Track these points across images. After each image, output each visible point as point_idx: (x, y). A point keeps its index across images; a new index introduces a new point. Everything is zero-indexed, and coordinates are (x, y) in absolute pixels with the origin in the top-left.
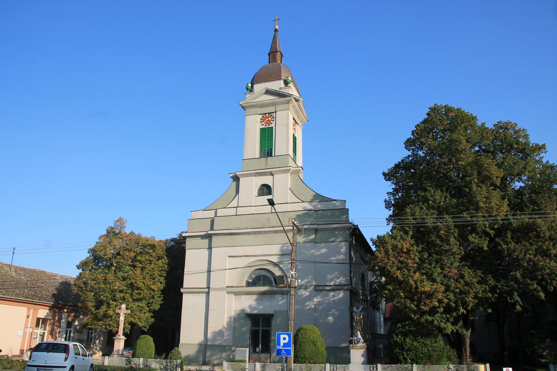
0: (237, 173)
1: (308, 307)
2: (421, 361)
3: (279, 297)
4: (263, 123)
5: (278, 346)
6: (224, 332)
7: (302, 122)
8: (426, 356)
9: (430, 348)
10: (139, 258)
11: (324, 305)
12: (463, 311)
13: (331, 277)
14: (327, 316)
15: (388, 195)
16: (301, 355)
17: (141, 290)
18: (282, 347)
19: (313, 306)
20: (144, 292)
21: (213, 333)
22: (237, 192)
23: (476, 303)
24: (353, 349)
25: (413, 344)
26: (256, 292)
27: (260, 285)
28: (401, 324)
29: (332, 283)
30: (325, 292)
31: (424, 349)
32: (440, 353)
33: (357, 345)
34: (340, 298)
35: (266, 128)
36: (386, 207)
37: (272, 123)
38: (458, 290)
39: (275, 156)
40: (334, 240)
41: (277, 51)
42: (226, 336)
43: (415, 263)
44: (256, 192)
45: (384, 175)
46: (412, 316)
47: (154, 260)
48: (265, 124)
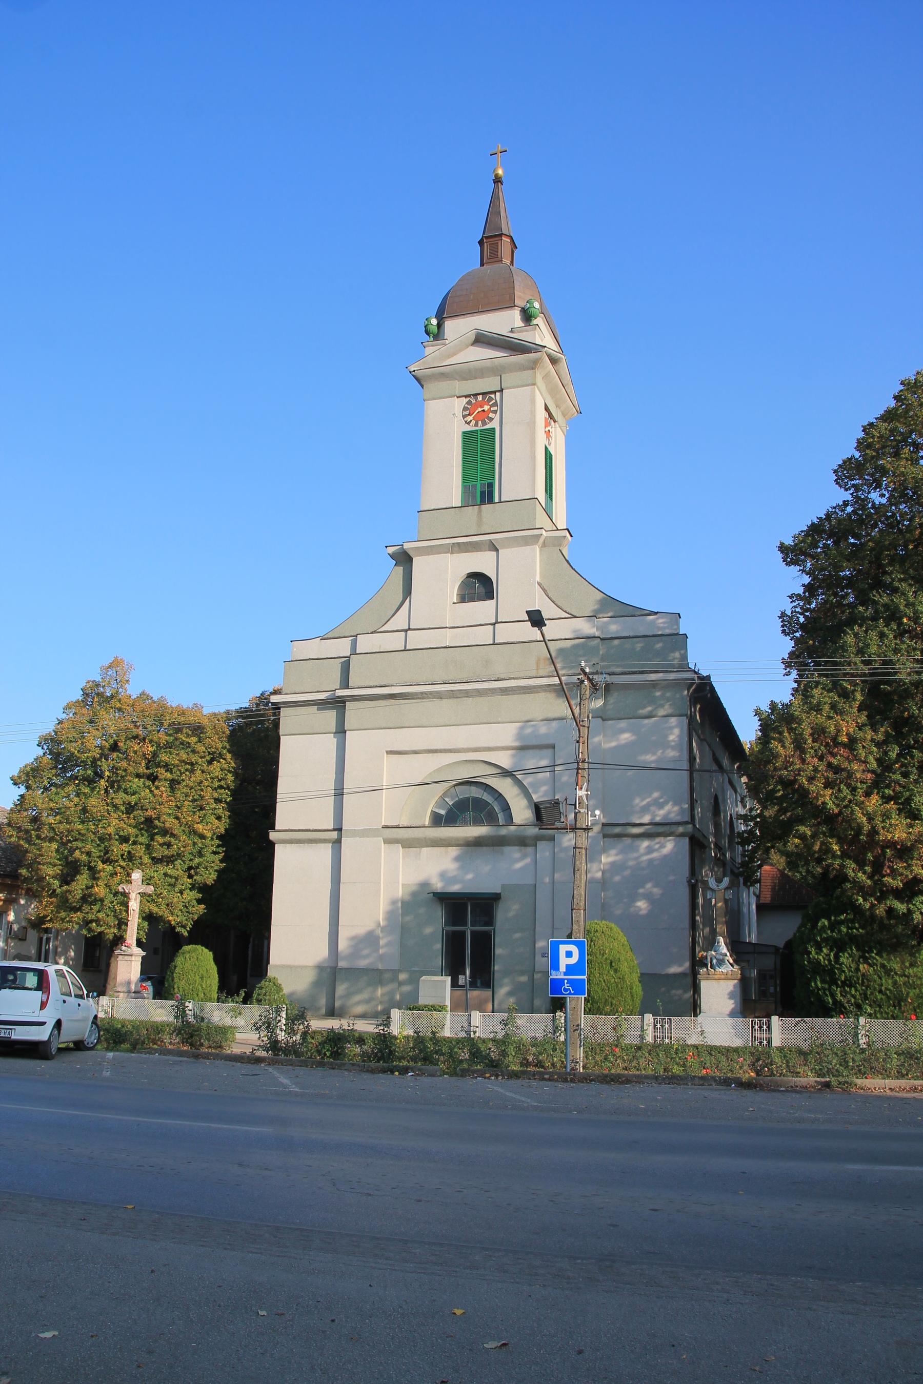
3: (514, 852)
4: (469, 418)
5: (553, 972)
6: (378, 938)
7: (564, 417)
8: (889, 998)
9: (900, 980)
10: (164, 757)
11: (627, 873)
13: (644, 803)
14: (634, 898)
15: (791, 602)
17: (173, 835)
18: (562, 974)
19: (599, 875)
20: (180, 841)
21: (352, 938)
22: (407, 591)
24: (707, 979)
25: (858, 970)
26: (457, 839)
27: (465, 823)
28: (829, 920)
29: (646, 819)
30: (628, 841)
31: (884, 981)
33: (718, 969)
34: (665, 856)
35: (477, 431)
36: (783, 631)
37: (491, 419)
39: (500, 502)
40: (651, 712)
41: (501, 235)
42: (383, 947)
43: (869, 771)
45: (782, 552)
46: (857, 900)
47: (200, 763)
48: (473, 422)
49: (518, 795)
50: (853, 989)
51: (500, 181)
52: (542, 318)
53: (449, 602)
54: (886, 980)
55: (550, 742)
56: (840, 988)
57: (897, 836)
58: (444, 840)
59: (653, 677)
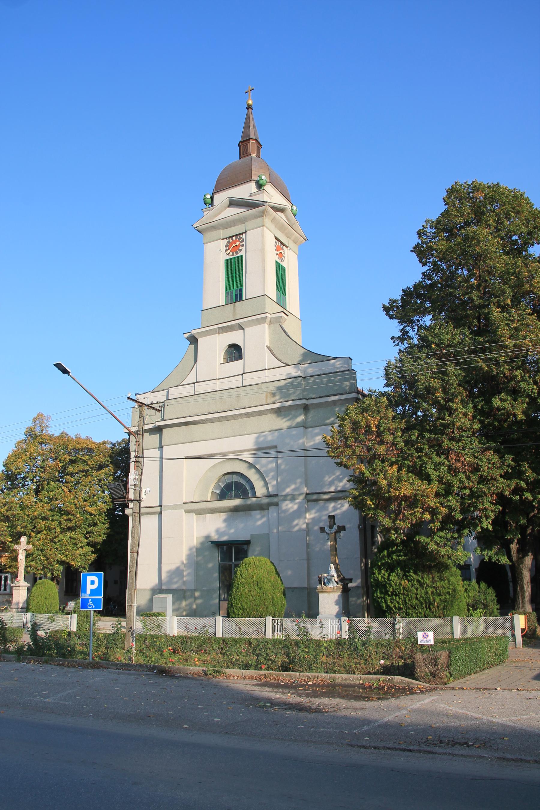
0: (193, 332)
1: (296, 529)
2: (414, 610)
3: (257, 514)
5: (83, 594)
6: (183, 571)
8: (422, 603)
9: (430, 590)
10: (70, 469)
12: (487, 526)
13: (331, 479)
15: (393, 342)
16: (237, 603)
18: (88, 595)
19: (304, 526)
20: (77, 518)
21: (168, 572)
22: (196, 360)
23: (499, 511)
24: (322, 592)
25: (400, 584)
26: (224, 508)
27: (231, 498)
28: (388, 551)
29: (332, 489)
30: (321, 503)
31: (419, 591)
32: (448, 596)
33: (328, 586)
34: (344, 512)
35: (233, 258)
37: (240, 250)
38: (468, 492)
39: (246, 300)
40: (334, 421)
41: (249, 140)
42: (185, 576)
44: (221, 355)
46: (391, 537)
48: (231, 253)
49: (258, 479)
50: (397, 597)
51: (250, 108)
52: (271, 185)
53: (218, 364)
54: (420, 591)
55: (274, 444)
56: (390, 596)
57: (402, 492)
58: (217, 509)
59: (333, 398)
